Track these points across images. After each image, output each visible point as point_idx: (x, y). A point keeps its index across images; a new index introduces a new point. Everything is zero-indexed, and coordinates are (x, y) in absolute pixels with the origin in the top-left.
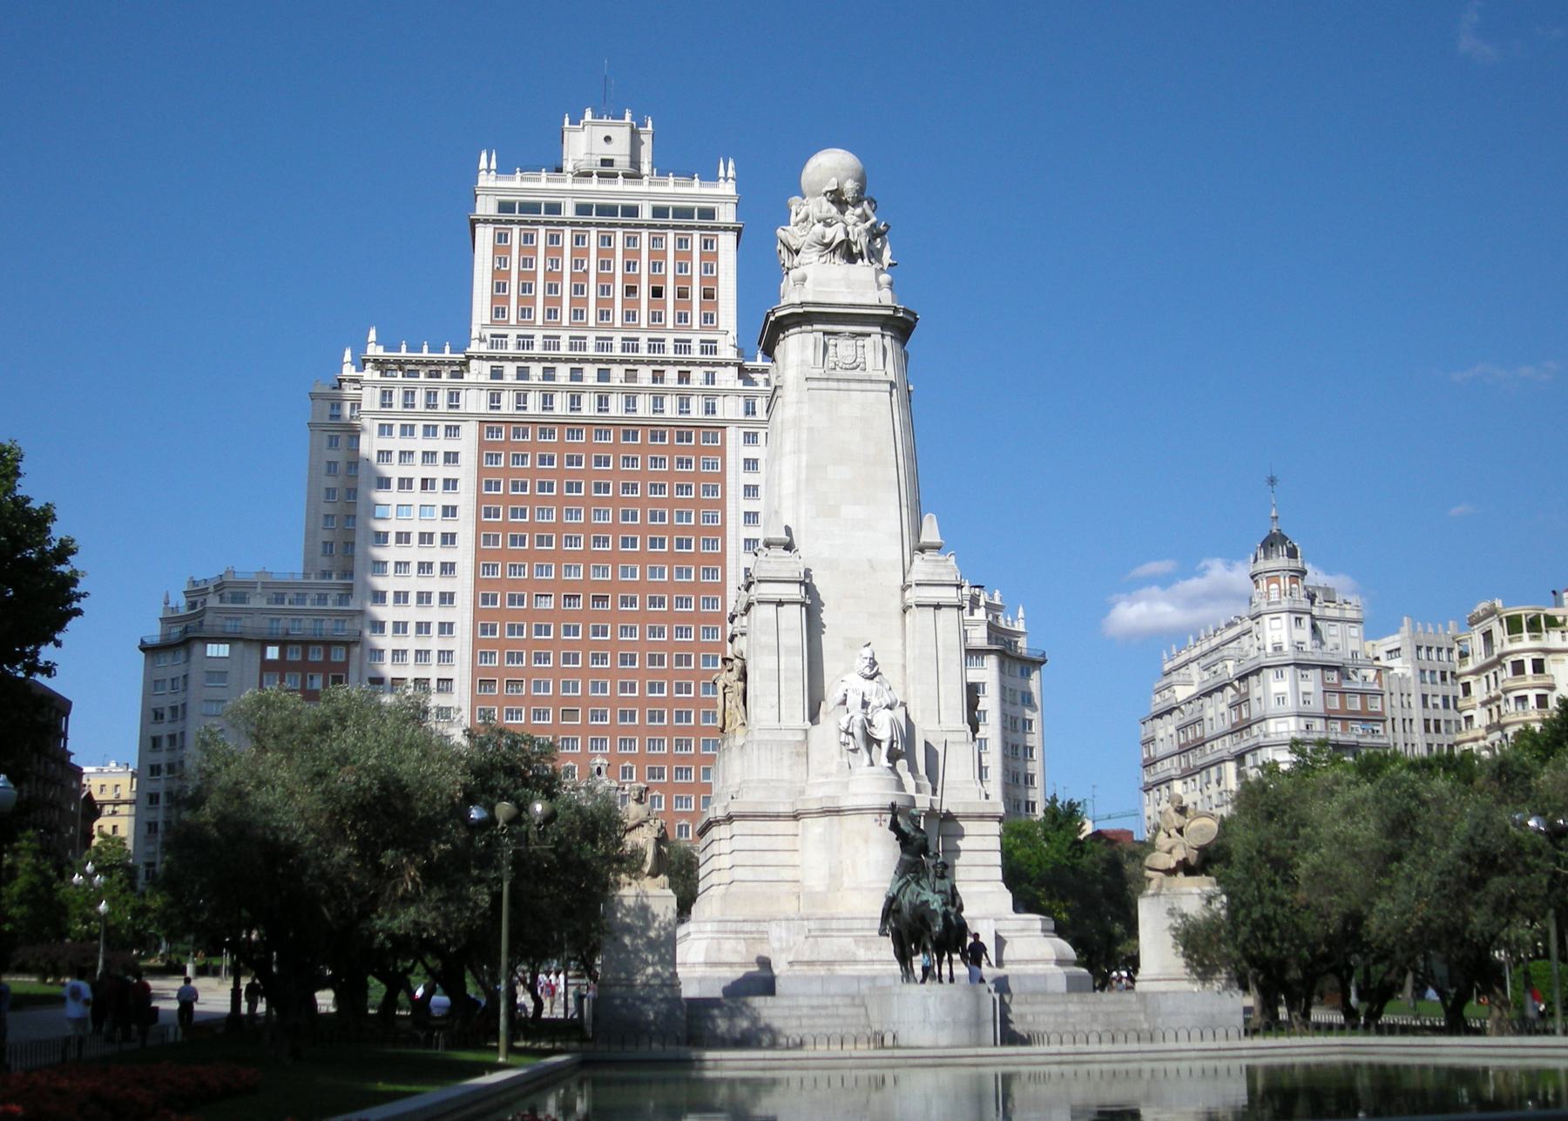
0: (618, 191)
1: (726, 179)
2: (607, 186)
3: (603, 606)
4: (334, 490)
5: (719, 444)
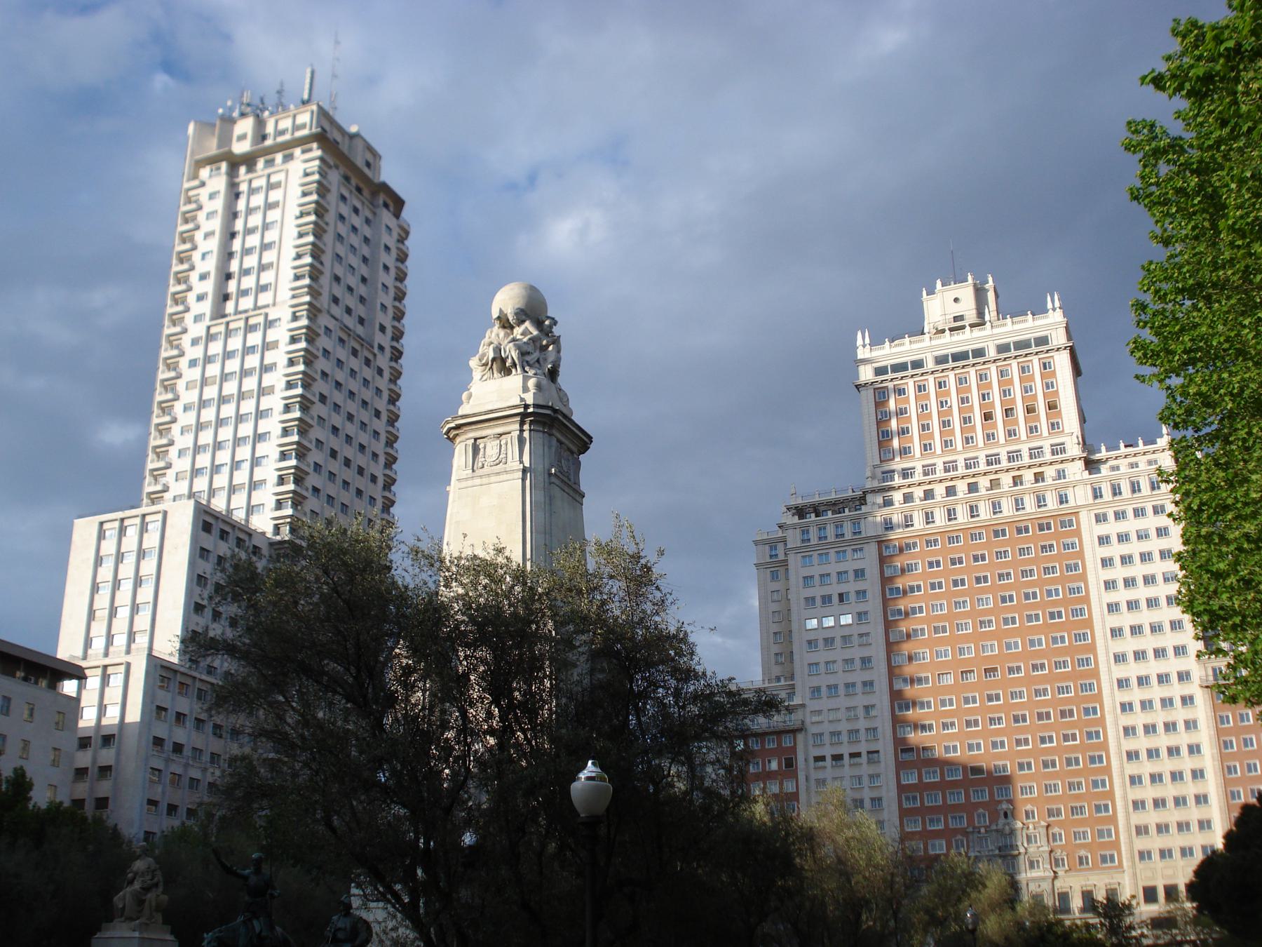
0: (967, 340)
1: (1054, 309)
2: (959, 337)
3: (994, 676)
4: (779, 612)
5: (1075, 527)
